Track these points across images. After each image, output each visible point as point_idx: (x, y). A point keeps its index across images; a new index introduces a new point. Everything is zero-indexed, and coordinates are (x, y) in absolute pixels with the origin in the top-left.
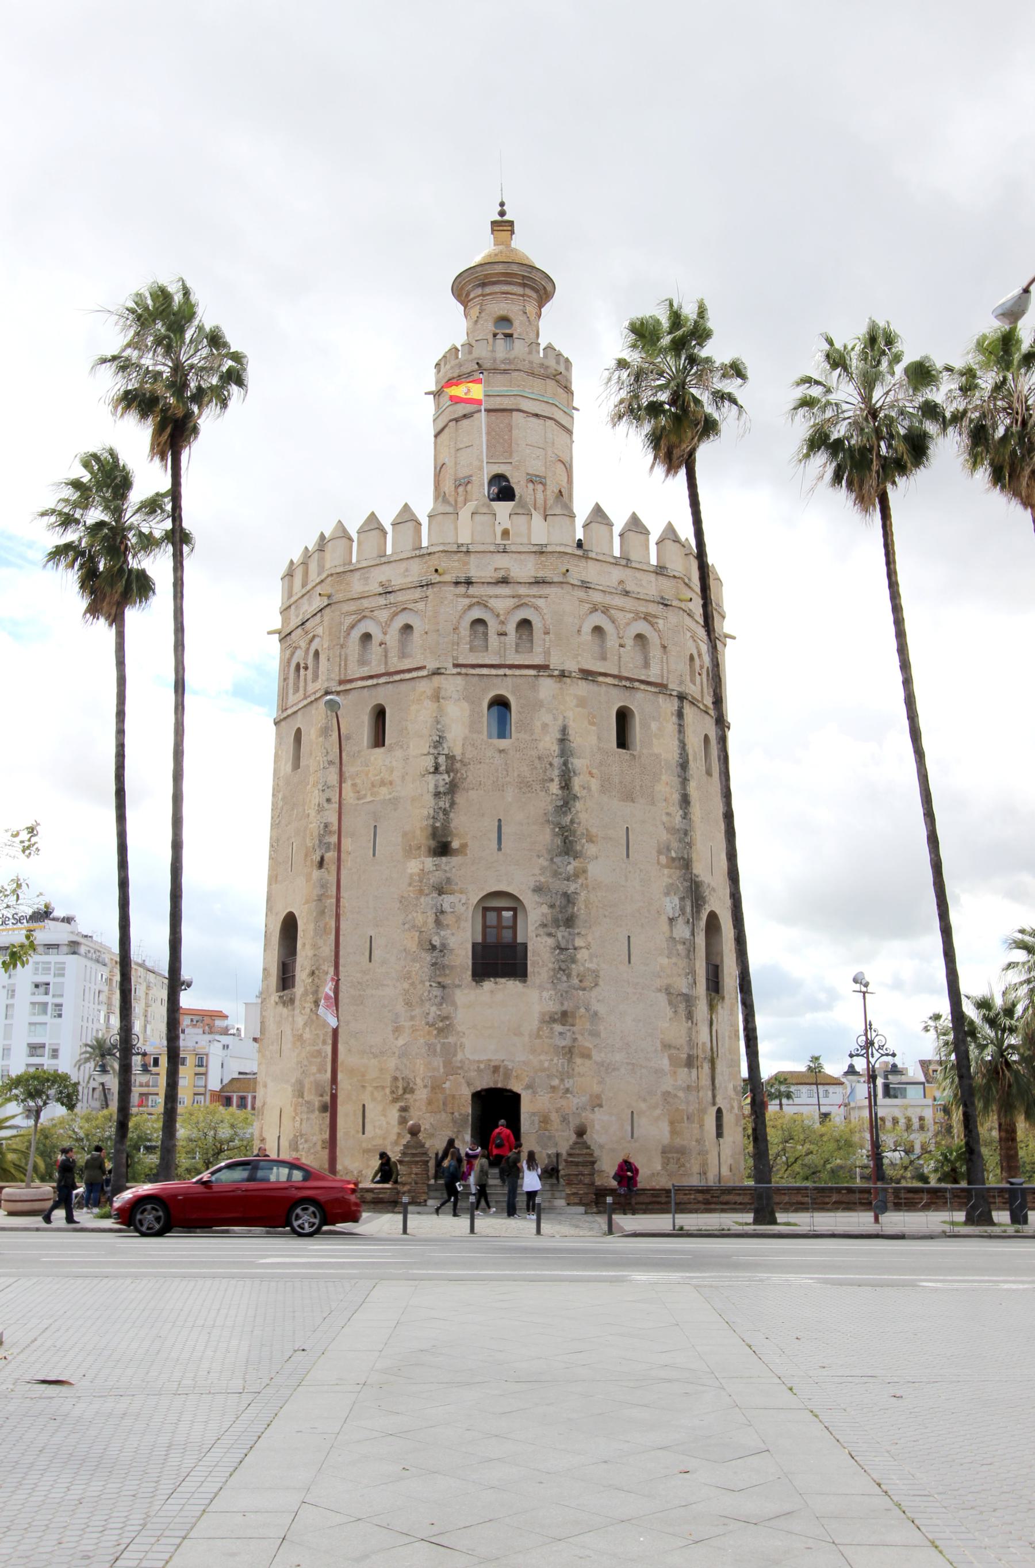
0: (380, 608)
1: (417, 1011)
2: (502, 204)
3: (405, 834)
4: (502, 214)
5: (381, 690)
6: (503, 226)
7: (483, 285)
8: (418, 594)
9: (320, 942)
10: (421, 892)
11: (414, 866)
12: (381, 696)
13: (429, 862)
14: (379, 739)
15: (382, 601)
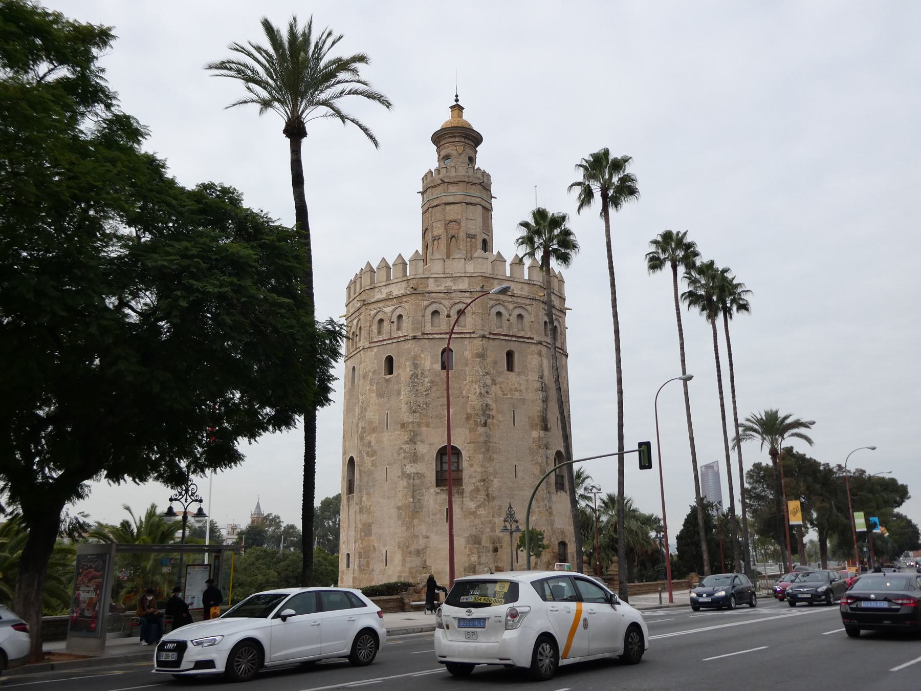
0: (508, 302)
1: (541, 504)
2: (457, 96)
3: (529, 418)
4: (457, 100)
5: (512, 343)
6: (457, 108)
7: (465, 138)
8: (528, 302)
9: (488, 465)
10: (540, 447)
11: (535, 434)
12: (513, 346)
13: (542, 433)
14: (510, 367)
15: (510, 299)
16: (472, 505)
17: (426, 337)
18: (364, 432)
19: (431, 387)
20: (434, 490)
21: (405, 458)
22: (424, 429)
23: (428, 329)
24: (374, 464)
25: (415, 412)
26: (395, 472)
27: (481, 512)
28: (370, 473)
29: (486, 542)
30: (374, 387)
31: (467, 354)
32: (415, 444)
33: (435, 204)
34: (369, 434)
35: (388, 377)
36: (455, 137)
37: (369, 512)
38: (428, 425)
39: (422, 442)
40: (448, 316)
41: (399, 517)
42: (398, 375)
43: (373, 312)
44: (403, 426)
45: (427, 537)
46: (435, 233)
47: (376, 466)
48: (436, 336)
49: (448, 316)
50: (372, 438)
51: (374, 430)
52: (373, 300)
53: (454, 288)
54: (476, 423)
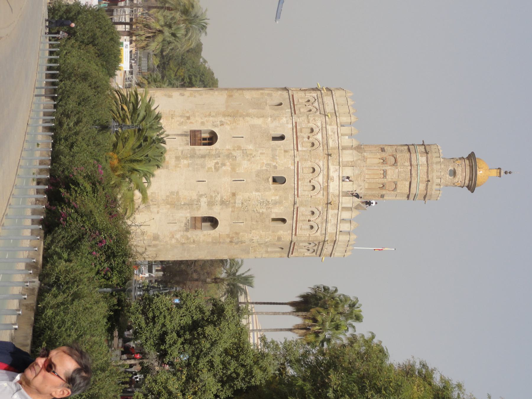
0: (318, 247)
2: (510, 173)
16: (178, 236)
17: (295, 210)
18: (233, 160)
19: (259, 213)
20: (189, 216)
21: (211, 197)
22: (230, 209)
23: (301, 209)
24: (210, 169)
25: (242, 203)
26: (202, 188)
27: (174, 241)
28: (203, 166)
29: (154, 242)
30: (264, 168)
31: (281, 233)
32: (220, 205)
33: (413, 172)
34: (231, 164)
35: (271, 180)
36: (469, 181)
37: (176, 166)
38: (233, 211)
39: (222, 209)
40: (309, 221)
41: (172, 193)
42: (270, 189)
43: (321, 164)
44: (234, 195)
45: (158, 213)
46: (389, 172)
47: (207, 171)
48: (295, 215)
49: (309, 221)
50: (228, 168)
51: (233, 169)
52: (330, 164)
53: (329, 225)
54: (233, 238)
